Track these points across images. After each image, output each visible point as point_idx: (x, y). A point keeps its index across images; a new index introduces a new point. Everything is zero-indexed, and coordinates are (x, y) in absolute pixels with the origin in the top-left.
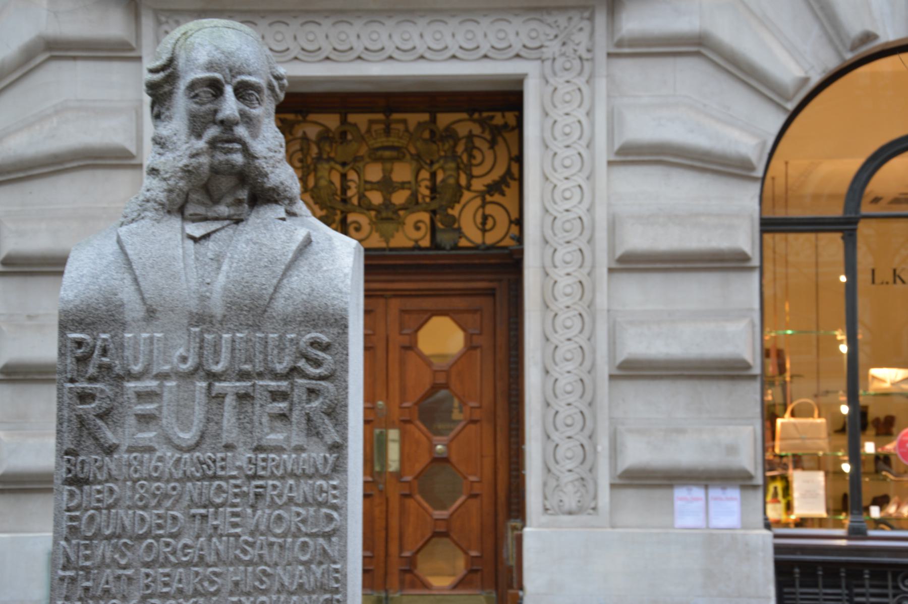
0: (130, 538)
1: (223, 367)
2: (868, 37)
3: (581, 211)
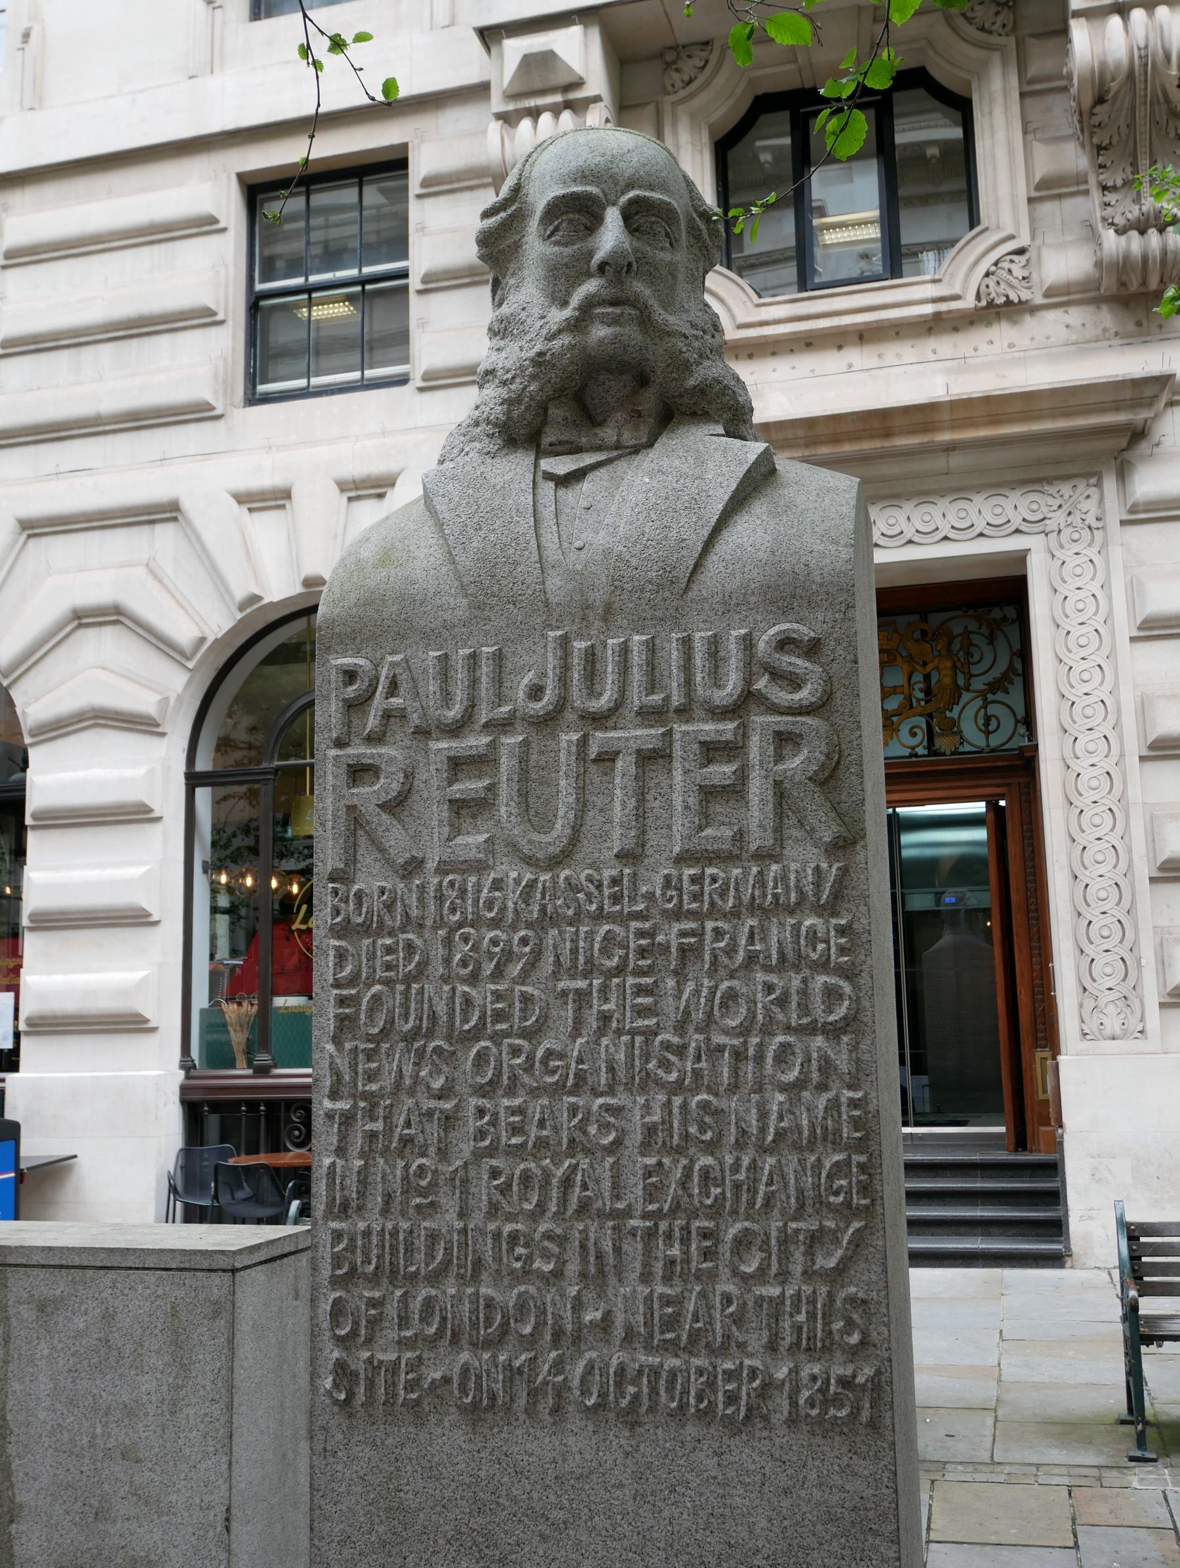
1: (609, 701)
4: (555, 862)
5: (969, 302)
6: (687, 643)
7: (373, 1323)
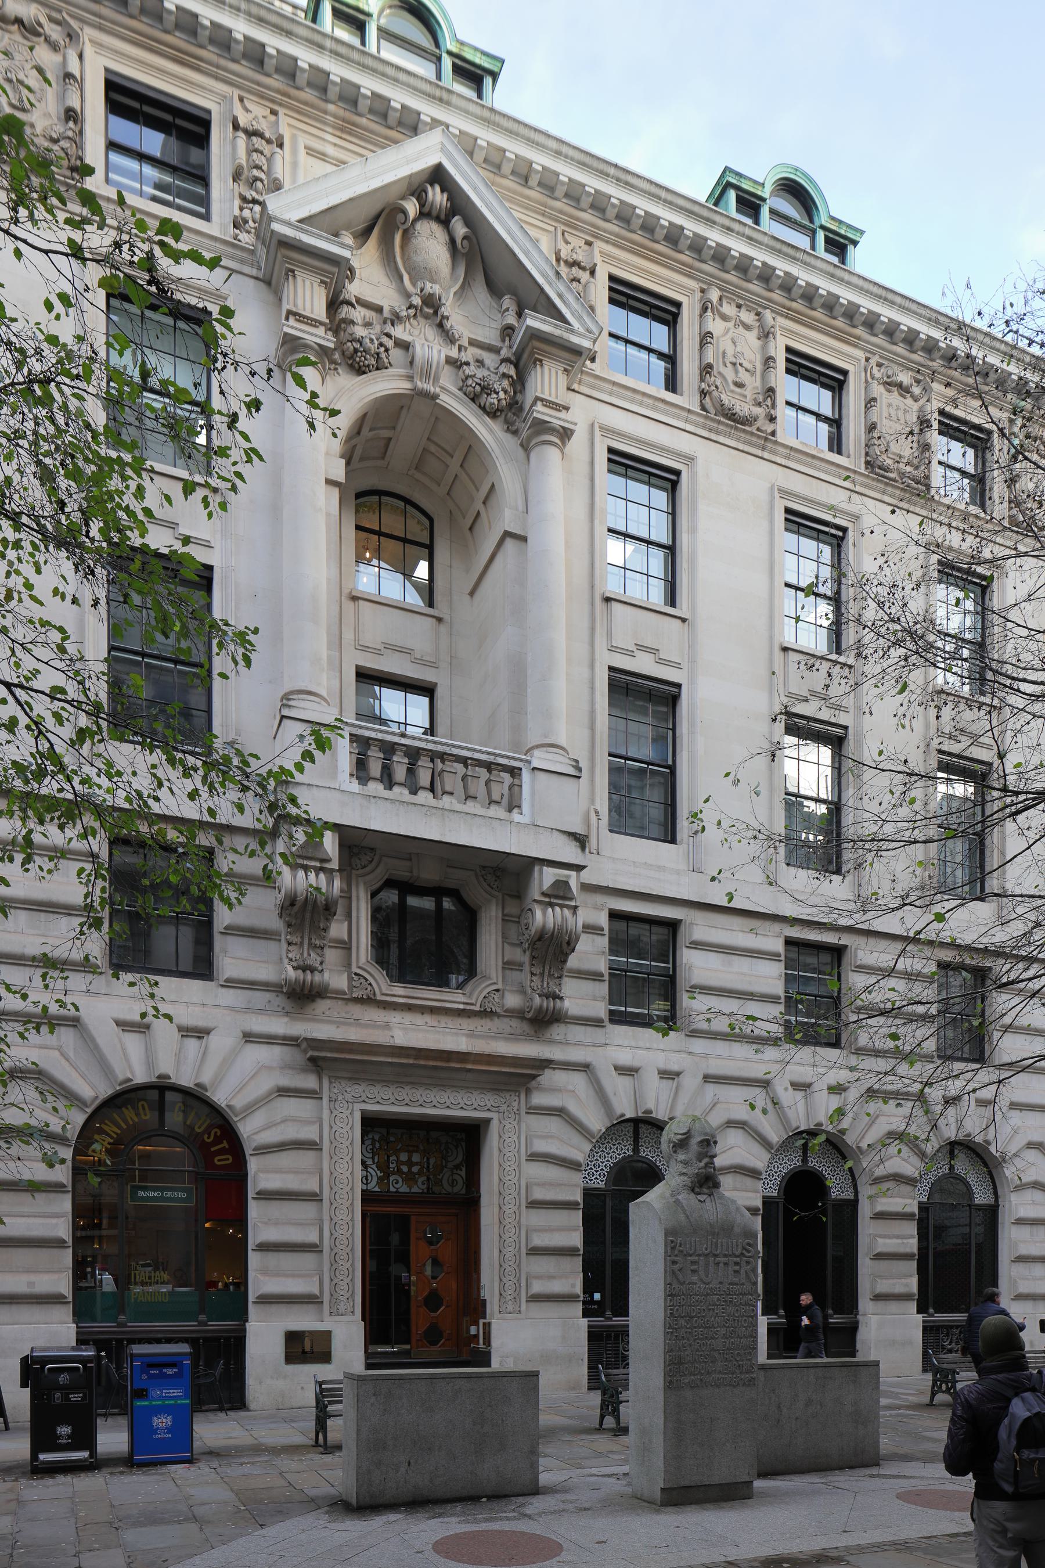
2: (623, 1115)
3: (515, 1180)
5: (477, 1008)
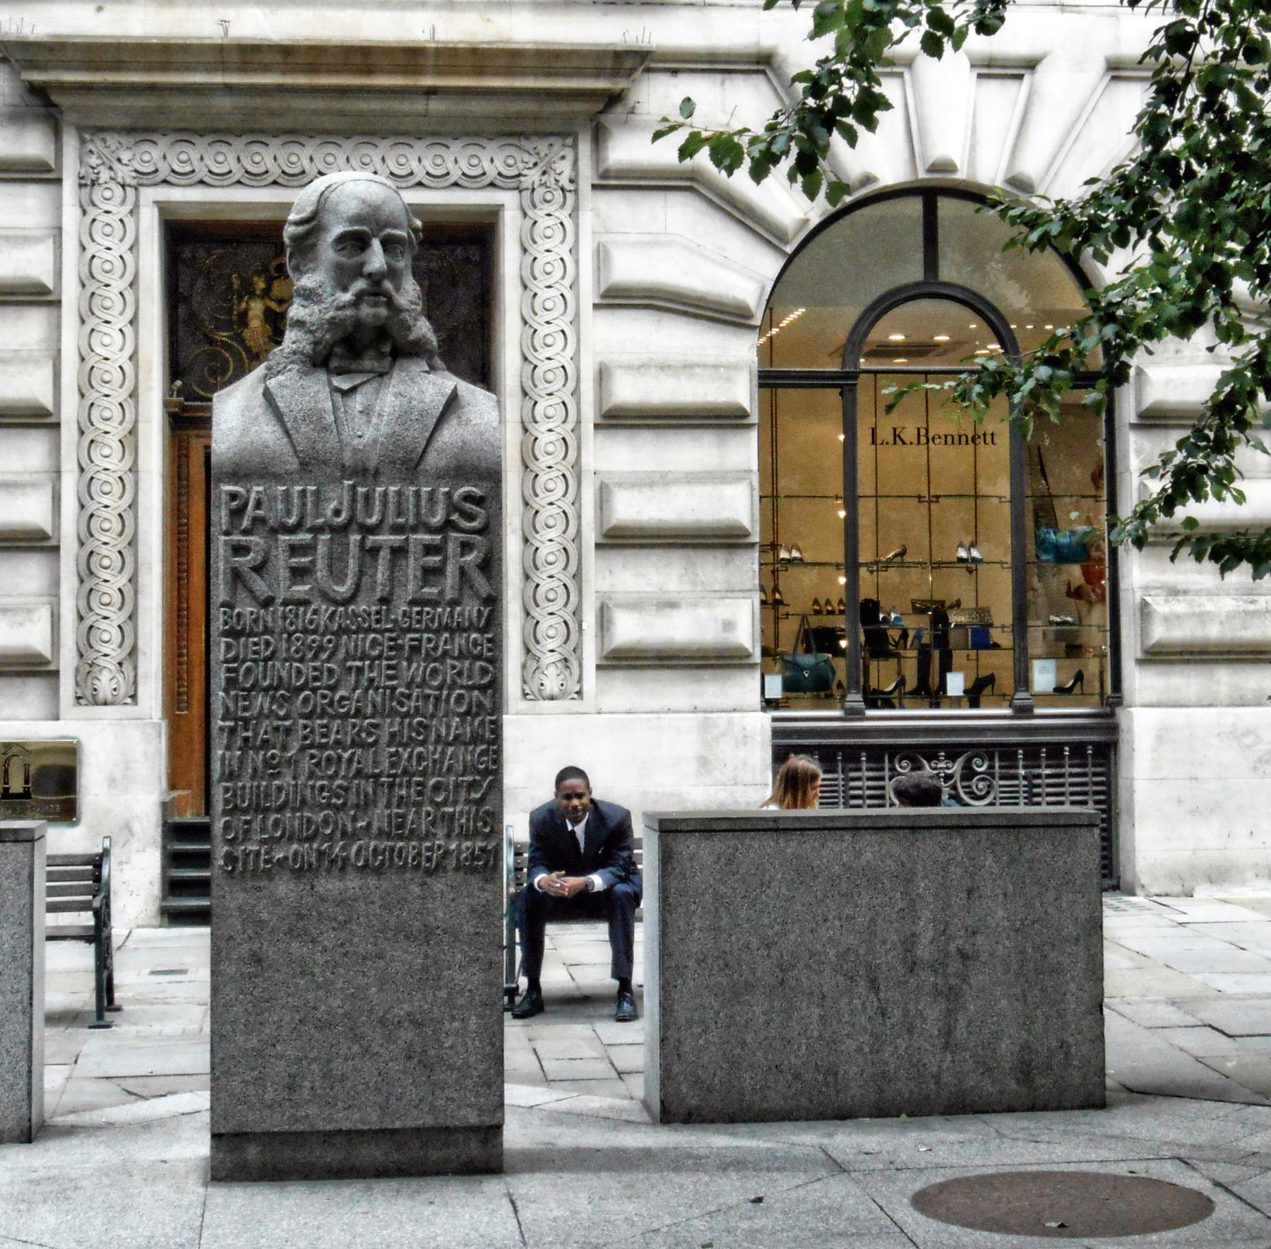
0: (287, 690)
3: (565, 358)
4: (346, 602)
6: (417, 494)
7: (247, 832)
